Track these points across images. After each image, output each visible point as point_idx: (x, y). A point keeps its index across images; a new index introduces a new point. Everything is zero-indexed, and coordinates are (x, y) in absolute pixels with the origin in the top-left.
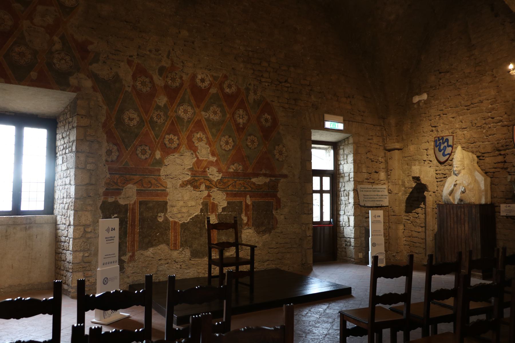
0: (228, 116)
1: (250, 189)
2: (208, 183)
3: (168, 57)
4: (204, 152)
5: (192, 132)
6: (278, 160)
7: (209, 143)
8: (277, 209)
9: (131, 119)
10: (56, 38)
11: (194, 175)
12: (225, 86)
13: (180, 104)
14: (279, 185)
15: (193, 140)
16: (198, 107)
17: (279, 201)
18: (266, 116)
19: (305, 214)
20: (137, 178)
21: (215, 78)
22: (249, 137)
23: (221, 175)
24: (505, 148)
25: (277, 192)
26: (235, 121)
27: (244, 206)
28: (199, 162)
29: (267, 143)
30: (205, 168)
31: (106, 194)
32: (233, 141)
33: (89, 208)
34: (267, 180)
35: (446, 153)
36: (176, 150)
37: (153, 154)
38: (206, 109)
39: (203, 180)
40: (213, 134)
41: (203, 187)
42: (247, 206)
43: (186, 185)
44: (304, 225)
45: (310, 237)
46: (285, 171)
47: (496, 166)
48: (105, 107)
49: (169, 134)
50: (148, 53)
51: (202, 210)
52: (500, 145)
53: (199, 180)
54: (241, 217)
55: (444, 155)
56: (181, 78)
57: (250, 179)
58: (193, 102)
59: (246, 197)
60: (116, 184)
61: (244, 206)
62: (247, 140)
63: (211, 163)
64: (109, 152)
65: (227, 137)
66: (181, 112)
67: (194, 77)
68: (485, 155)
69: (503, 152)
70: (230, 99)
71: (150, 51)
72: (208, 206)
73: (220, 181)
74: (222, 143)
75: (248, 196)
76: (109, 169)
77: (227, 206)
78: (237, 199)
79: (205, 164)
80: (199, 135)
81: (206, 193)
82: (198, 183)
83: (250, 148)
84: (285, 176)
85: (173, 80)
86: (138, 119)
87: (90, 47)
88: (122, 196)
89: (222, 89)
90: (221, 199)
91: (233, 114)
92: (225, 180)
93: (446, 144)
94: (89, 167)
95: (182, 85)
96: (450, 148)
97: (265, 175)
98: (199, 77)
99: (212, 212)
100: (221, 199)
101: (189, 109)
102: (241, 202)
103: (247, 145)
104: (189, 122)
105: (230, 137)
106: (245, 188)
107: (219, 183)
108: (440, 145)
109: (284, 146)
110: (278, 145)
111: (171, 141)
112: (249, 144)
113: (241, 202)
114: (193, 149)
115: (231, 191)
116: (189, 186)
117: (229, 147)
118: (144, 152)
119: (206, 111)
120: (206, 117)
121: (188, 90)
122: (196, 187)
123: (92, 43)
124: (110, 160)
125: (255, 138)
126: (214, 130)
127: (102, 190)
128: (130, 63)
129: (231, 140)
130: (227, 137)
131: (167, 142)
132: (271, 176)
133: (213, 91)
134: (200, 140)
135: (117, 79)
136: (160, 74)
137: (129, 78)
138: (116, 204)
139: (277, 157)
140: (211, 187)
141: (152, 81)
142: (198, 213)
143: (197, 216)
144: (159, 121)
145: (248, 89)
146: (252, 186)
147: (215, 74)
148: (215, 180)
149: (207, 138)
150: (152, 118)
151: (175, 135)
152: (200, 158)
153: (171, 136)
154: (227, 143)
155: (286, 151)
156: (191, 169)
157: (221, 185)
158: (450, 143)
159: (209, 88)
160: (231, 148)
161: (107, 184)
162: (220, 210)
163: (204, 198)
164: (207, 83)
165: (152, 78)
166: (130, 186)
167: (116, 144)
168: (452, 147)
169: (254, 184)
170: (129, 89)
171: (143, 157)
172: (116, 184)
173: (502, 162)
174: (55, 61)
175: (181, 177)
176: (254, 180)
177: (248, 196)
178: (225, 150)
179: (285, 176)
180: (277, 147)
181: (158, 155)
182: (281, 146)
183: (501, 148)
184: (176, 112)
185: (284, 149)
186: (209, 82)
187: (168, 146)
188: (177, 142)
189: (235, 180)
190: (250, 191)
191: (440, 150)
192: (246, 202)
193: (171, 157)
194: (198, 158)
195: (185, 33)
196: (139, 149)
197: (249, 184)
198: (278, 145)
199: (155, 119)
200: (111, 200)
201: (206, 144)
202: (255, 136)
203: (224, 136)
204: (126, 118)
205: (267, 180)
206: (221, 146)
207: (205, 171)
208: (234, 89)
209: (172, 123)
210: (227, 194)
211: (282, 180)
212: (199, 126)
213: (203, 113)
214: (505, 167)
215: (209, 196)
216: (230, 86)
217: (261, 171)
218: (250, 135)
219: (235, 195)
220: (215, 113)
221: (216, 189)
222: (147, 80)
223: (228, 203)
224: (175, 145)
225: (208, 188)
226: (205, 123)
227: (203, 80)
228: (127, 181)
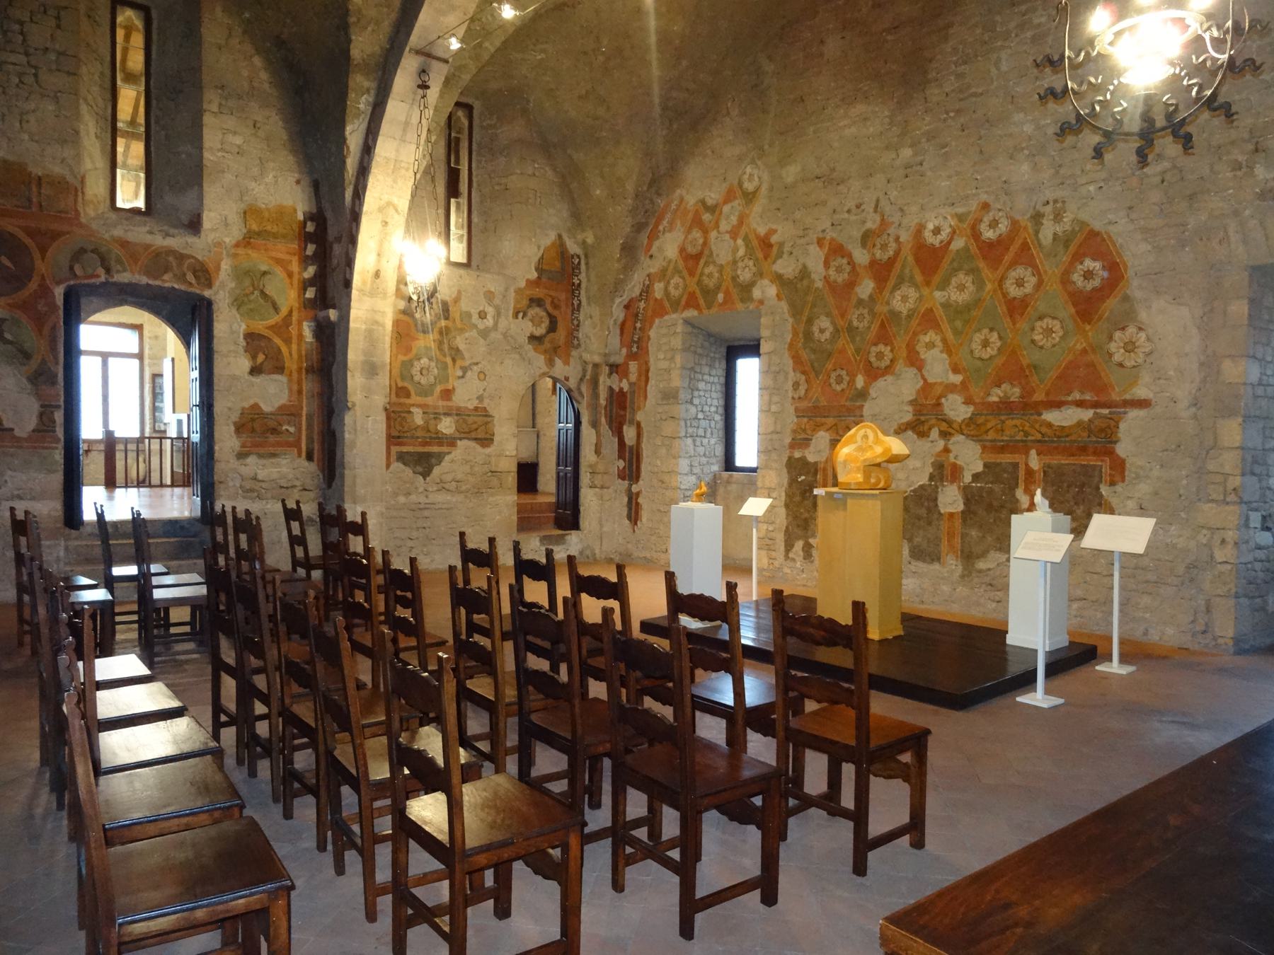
0: (989, 286)
1: (1039, 437)
2: (944, 426)
3: (875, 211)
4: (938, 367)
5: (915, 334)
6: (1121, 365)
7: (948, 349)
8: (1112, 484)
9: (822, 331)
10: (740, 242)
11: (918, 412)
12: (983, 227)
13: (896, 287)
14: (1122, 426)
15: (917, 348)
16: (928, 283)
17: (1119, 466)
18: (1089, 264)
19: (1213, 501)
20: (830, 421)
21: (960, 217)
22: (1038, 324)
23: (971, 409)
25: (1116, 442)
26: (1005, 295)
27: (1022, 473)
28: (927, 387)
29: (1088, 327)
30: (939, 398)
31: (793, 446)
32: (1000, 338)
33: (774, 465)
34: (1087, 414)
36: (888, 370)
37: (852, 382)
38: (943, 285)
39: (933, 421)
40: (957, 333)
41: (935, 433)
42: (1030, 473)
43: (905, 430)
44: (1205, 531)
45: (1229, 567)
46: (1141, 392)
48: (791, 320)
49: (875, 344)
50: (846, 215)
51: (931, 478)
53: (927, 421)
54: (1014, 496)
56: (897, 239)
57: (1040, 414)
58: (919, 278)
59: (1027, 454)
60: (804, 431)
61: (1022, 473)
62: (1033, 329)
63: (951, 388)
64: (796, 385)
65: (986, 331)
66: (897, 303)
67: (920, 228)
70: (992, 251)
71: (849, 211)
72: (944, 471)
73: (971, 421)
74: (974, 346)
75: (1033, 452)
76: (797, 410)
77: (983, 472)
78: (1006, 458)
79: (939, 390)
80: (931, 336)
81: (941, 443)
82: (926, 428)
83: (1041, 347)
84: (1143, 404)
85: (884, 247)
86: (831, 329)
87: (774, 239)
88: (812, 449)
89: (976, 235)
90: (970, 457)
91: (1001, 281)
92: (981, 420)
94: (774, 408)
95: (897, 253)
97: (1080, 404)
98: (930, 226)
99: (952, 482)
100: (970, 457)
101: (912, 293)
102: (1015, 466)
103: (1033, 341)
104: (909, 317)
105: (992, 330)
106: (1026, 434)
107: (968, 425)
109: (1140, 329)
110: (1123, 329)
111: (880, 356)
112: (1037, 338)
113: (1015, 466)
114: (915, 361)
115: (994, 441)
116: (910, 433)
117: (990, 351)
118: (839, 380)
119: (943, 289)
120: (943, 300)
121: (910, 259)
122: (922, 435)
123: (775, 231)
124: (796, 396)
125: (1056, 322)
126: (958, 324)
127: (788, 440)
128: (820, 242)
129: (994, 337)
130: (986, 331)
131: (873, 359)
132: (1095, 405)
133: (958, 244)
134: (931, 345)
135: (804, 273)
136: (864, 245)
137: (820, 268)
138: (803, 459)
139: (1117, 358)
140: (950, 434)
141: (851, 262)
142: (924, 480)
143: (921, 486)
144: (861, 325)
145: (1037, 218)
146: (1044, 430)
147: (960, 210)
148: (959, 420)
149: (944, 341)
150: (850, 322)
151: (886, 345)
152: (930, 380)
153: (881, 347)
154: (986, 344)
155: (1148, 339)
156: (912, 403)
157: (972, 428)
159: (949, 243)
160: (995, 352)
161: (794, 431)
162: (967, 478)
163: (938, 455)
164: (944, 235)
165: (850, 256)
166: (822, 433)
167: (803, 373)
169: (1050, 425)
170: (819, 284)
171: (839, 388)
172: (804, 431)
174: (739, 272)
175: (896, 417)
176: (1052, 416)
177: (1033, 452)
178: (981, 359)
179: (1143, 404)
180: (1117, 335)
181: (860, 381)
182: (1131, 330)
184: (888, 303)
185: (1143, 335)
186: (948, 230)
187: (875, 365)
188: (891, 356)
189: (1003, 418)
190: (1039, 441)
192: (1027, 465)
193: (881, 383)
194: (925, 380)
195: (907, 153)
196: (833, 375)
197: (1037, 426)
198: (1123, 329)
199: (855, 323)
200: (797, 455)
201: (942, 352)
202: (1054, 318)
203: (979, 330)
204: (815, 329)
205: (1087, 414)
206: (972, 352)
207: (939, 405)
208: (1003, 227)
209: (882, 325)
210: (984, 448)
211: (1133, 414)
212: (929, 320)
213: (938, 294)
215: (946, 450)
216: (994, 224)
217: (1068, 395)
218: (1040, 318)
219: (1002, 450)
220: (961, 288)
221: (961, 438)
222: (845, 261)
223: (985, 465)
224: (886, 362)
225: (945, 435)
226: (939, 312)
227: (937, 231)
228: (818, 427)
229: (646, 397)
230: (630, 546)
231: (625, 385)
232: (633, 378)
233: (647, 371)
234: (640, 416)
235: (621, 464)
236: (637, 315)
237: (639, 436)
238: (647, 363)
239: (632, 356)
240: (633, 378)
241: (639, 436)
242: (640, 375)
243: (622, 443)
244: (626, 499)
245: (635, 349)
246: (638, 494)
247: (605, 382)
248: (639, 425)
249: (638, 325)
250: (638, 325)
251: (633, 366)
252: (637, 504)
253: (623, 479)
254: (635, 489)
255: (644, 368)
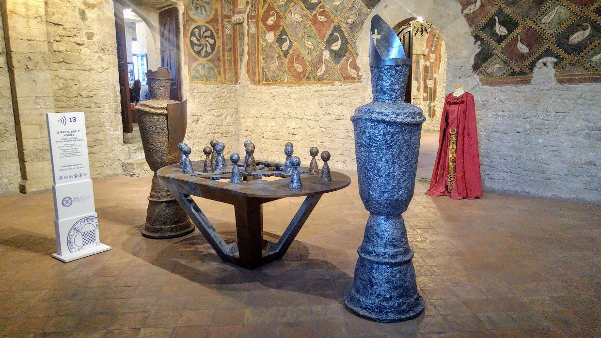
229: (439, 68)
230: (429, 126)
231: (428, 64)
232: (432, 60)
233: (440, 57)
234: (435, 76)
235: (425, 95)
236: (435, 35)
237: (435, 83)
238: (440, 55)
239: (431, 52)
240: (432, 60)
241: (435, 83)
242: (436, 59)
243: (426, 87)
244: (428, 109)
245: (433, 49)
246: (434, 106)
247: (422, 62)
248: (435, 79)
249: (435, 39)
250: (435, 39)
251: (432, 56)
252: (434, 110)
253: (427, 100)
254: (432, 104)
255: (438, 56)
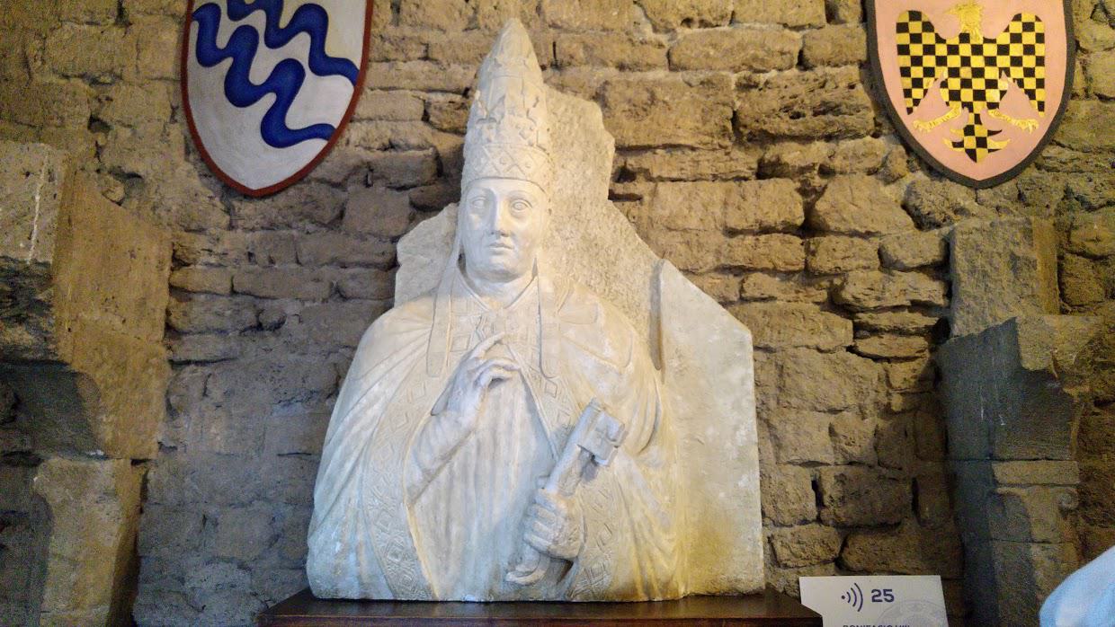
24: (812, 122)
35: (296, 118)
47: (742, 250)
52: (772, 100)
55: (276, 133)
68: (657, 163)
69: (792, 154)
93: (299, 47)
96: (340, 87)
108: (244, 44)
158: (344, 40)
168: (356, 76)
173: (788, 229)
183: (783, 125)
191: (239, 92)
214: (823, 262)
